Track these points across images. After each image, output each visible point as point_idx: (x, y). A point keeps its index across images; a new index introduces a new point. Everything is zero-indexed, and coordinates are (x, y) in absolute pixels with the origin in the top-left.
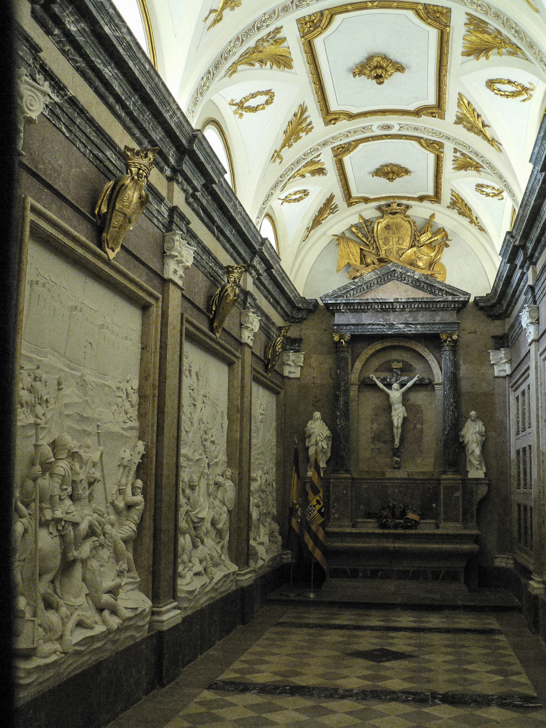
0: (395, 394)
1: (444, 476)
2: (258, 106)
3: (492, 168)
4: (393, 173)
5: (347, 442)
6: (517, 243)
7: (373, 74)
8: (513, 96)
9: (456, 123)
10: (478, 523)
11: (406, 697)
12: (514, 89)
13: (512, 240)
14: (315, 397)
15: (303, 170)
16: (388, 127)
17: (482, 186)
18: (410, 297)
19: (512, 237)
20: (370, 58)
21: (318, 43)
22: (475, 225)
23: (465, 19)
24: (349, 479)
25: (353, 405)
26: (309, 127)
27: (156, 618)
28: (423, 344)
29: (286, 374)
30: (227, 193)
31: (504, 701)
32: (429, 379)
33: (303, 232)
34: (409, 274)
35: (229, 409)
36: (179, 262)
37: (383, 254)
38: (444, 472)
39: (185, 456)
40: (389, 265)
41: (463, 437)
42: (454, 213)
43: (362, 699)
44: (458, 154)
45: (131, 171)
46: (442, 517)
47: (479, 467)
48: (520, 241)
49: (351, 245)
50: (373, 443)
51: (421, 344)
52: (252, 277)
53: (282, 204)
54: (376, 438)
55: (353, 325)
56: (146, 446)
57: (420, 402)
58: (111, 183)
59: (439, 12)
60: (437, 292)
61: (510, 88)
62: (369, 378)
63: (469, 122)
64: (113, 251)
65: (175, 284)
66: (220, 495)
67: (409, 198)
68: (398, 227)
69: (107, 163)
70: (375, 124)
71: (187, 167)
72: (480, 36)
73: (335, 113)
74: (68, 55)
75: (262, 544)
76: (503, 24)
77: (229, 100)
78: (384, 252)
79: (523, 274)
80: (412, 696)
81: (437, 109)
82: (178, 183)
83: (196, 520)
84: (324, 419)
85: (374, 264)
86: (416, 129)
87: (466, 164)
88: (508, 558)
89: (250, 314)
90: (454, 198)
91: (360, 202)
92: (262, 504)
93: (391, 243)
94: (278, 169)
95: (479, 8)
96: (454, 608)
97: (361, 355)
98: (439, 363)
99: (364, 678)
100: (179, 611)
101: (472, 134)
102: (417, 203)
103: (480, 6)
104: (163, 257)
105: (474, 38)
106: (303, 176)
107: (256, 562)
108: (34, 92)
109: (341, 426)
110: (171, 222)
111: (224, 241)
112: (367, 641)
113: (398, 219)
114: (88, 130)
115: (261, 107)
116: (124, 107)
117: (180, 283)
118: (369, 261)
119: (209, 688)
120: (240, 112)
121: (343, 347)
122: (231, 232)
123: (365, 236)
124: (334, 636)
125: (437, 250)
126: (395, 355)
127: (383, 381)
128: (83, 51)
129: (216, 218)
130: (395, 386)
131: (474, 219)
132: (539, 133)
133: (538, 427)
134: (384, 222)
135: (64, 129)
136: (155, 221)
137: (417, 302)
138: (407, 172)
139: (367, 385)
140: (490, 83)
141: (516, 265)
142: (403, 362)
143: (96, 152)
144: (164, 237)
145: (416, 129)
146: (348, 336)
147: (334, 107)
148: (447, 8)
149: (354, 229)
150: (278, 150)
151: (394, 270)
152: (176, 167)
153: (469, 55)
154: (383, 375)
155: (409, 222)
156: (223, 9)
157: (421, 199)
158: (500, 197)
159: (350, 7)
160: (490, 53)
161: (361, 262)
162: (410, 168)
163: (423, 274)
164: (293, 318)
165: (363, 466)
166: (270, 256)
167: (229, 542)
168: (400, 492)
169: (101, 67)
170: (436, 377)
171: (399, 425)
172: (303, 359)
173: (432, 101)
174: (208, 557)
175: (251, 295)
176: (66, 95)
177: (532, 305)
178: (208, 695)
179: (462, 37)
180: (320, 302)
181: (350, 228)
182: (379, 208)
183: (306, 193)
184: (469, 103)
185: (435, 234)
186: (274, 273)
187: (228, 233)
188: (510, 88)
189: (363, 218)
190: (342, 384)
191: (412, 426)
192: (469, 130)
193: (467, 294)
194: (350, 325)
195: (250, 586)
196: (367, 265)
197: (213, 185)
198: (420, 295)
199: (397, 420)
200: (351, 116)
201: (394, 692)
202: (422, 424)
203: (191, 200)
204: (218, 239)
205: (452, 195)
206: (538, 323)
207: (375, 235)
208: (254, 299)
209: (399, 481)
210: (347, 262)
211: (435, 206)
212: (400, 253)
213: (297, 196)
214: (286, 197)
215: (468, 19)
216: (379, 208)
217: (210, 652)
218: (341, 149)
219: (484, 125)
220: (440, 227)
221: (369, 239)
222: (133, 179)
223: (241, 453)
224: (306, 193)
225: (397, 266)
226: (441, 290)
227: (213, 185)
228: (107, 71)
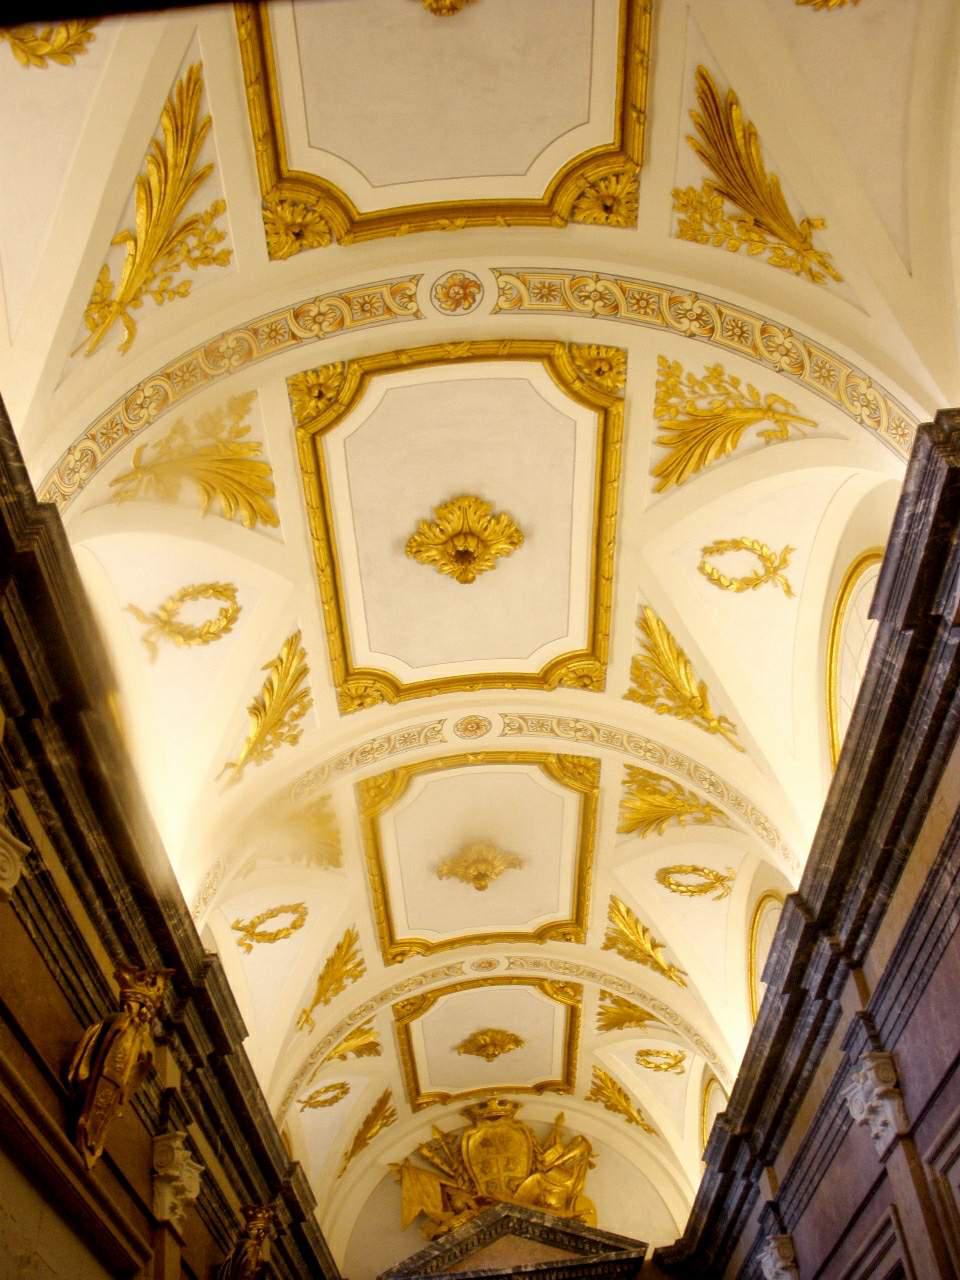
2: (279, 932)
3: (673, 1016)
4: (495, 1045)
6: (738, 1131)
7: (473, 872)
8: (701, 891)
9: (606, 947)
12: (702, 880)
13: (727, 1128)
15: (344, 1045)
16: (490, 965)
17: (648, 1053)
18: (541, 1261)
19: (727, 1121)
20: (466, 848)
21: (387, 824)
22: (637, 1123)
23: (622, 774)
26: (359, 969)
30: (244, 1072)
34: (534, 1220)
36: (179, 1191)
37: (482, 1191)
40: (498, 1208)
42: (598, 1109)
44: (608, 1002)
45: (130, 1007)
48: (742, 1127)
49: (424, 1178)
53: (302, 1110)
58: (97, 1027)
59: (581, 766)
60: (587, 1247)
61: (694, 880)
63: (629, 943)
64: (93, 1153)
65: (173, 1232)
67: (519, 1090)
68: (504, 1141)
69: (83, 996)
70: (467, 962)
71: (190, 1020)
72: (650, 798)
73: (403, 944)
74: (39, 807)
76: (690, 775)
77: (232, 921)
79: (748, 1188)
81: (573, 928)
82: (173, 1049)
85: (469, 1208)
86: (537, 964)
87: (623, 1015)
90: (597, 1081)
91: (435, 1102)
93: (495, 1170)
94: (307, 1043)
95: (648, 754)
101: (634, 964)
102: (534, 1097)
103: (649, 750)
104: (152, 1180)
105: (638, 804)
106: (343, 1057)
108: (7, 850)
110: (164, 1117)
111: (231, 1167)
113: (501, 1127)
114: (61, 935)
115: (285, 933)
116: (108, 903)
117: (179, 1230)
118: (459, 1204)
120: (248, 942)
123: (446, 1161)
125: (575, 1176)
128: (64, 801)
131: (635, 1114)
132: (779, 929)
134: (477, 1136)
135: (30, 926)
136: (142, 1112)
137: (554, 1269)
138: (517, 1042)
140: (663, 876)
141: (734, 1173)
143: (69, 973)
144: (152, 1143)
145: (537, 964)
147: (401, 934)
148: (593, 759)
149: (425, 1152)
150: (308, 1009)
151: (507, 1217)
152: (174, 1020)
153: (629, 831)
155: (524, 1132)
156: (246, 761)
157: (540, 1088)
158: (679, 1070)
159: (440, 764)
160: (664, 826)
161: (445, 1208)
162: (522, 1034)
163: (560, 1219)
169: (85, 831)
173: (564, 913)
176: (38, 867)
177: (779, 1235)
179: (618, 802)
182: (467, 1112)
183: (344, 1089)
184: (628, 911)
185: (569, 1147)
187: (238, 1150)
188: (694, 880)
192: (629, 956)
193: (644, 1245)
196: (457, 1212)
197: (226, 1057)
198: (558, 1256)
200: (429, 948)
203: (188, 1083)
205: (596, 1076)
206: (797, 1267)
210: (419, 1209)
212: (513, 1185)
213: (330, 1095)
214: (311, 1098)
215: (629, 775)
216: (467, 1112)
218: (408, 1007)
219: (654, 945)
220: (576, 1134)
221: (455, 1166)
222: (132, 1021)
224: (344, 1089)
225: (512, 1208)
226: (593, 1243)
227: (226, 1057)
228: (91, 838)
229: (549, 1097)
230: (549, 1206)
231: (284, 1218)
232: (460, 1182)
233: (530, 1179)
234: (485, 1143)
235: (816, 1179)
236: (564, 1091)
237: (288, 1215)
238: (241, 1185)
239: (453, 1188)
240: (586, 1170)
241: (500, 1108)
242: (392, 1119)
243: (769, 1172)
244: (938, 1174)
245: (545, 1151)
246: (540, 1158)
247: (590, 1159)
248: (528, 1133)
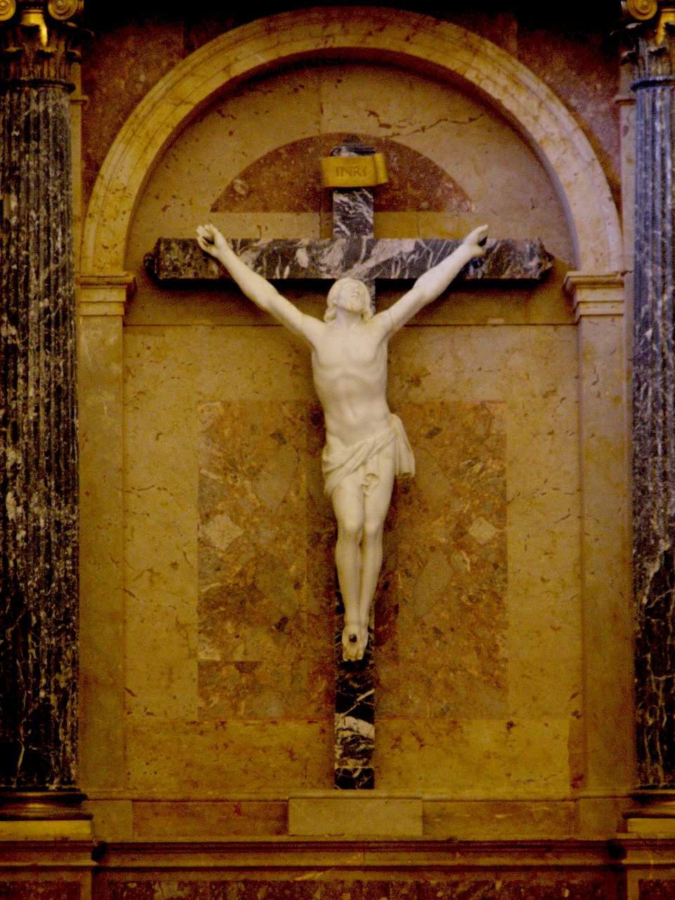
0: (347, 341)
1: (641, 827)
5: (67, 626)
24: (75, 846)
25: (96, 409)
28: (513, 45)
32: (546, 256)
38: (642, 802)
50: (209, 631)
51: (498, 41)
54: (231, 603)
57: (485, 391)
62: (188, 245)
97: (142, 108)
98: (605, 158)
109: (33, 537)
121: (42, 57)
126: (346, 107)
127: (273, 260)
130: (349, 291)
139: (179, 283)
142: (388, 147)
154: (275, 226)
165: (153, 774)
170: (585, 245)
171: (374, 526)
190: (37, 284)
191: (438, 531)
199: (359, 499)
202: (500, 515)
209: (371, 859)
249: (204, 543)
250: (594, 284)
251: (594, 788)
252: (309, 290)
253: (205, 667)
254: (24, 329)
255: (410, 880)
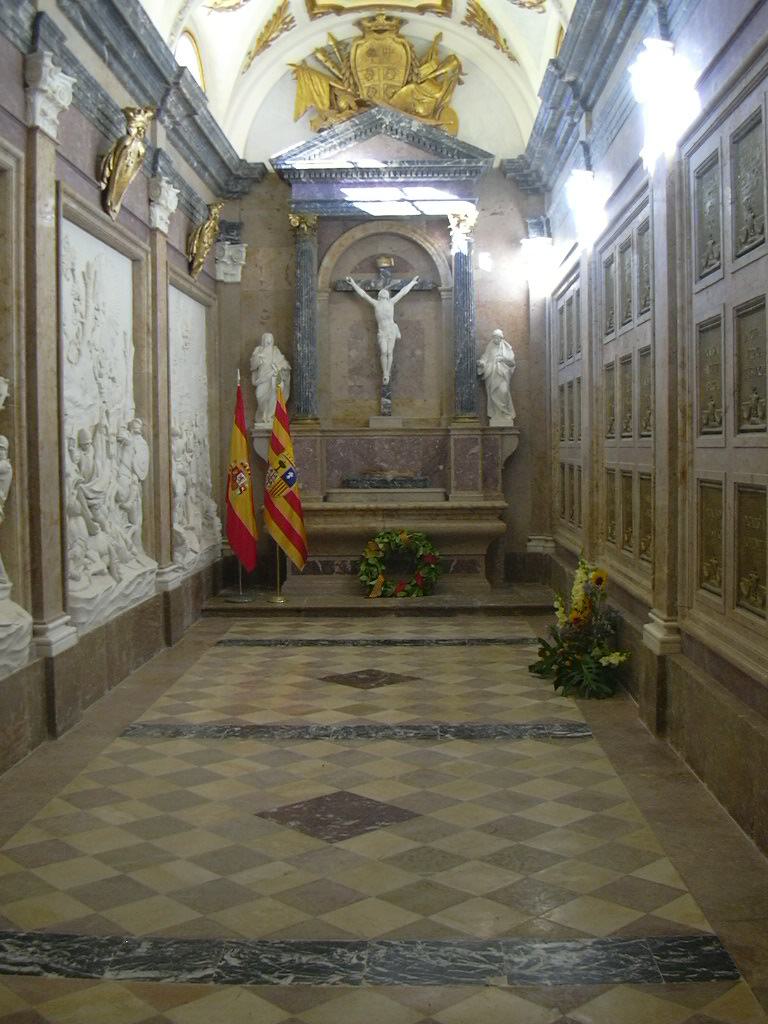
0: (385, 306)
1: (454, 425)
5: (313, 377)
10: (504, 490)
11: (406, 733)
14: (265, 311)
22: (503, 51)
27: (40, 639)
29: (220, 277)
31: (542, 732)
33: (241, 58)
34: (402, 124)
35: (136, 330)
37: (364, 95)
39: (71, 400)
40: (373, 111)
41: (482, 366)
42: (471, 33)
43: (344, 738)
46: (453, 483)
47: (505, 411)
49: (316, 79)
52: (166, 127)
54: (355, 371)
55: (320, 201)
56: (11, 386)
60: (445, 153)
65: (44, 134)
66: (127, 459)
67: (404, 9)
75: (192, 529)
78: (365, 92)
79: (573, 125)
80: (415, 732)
83: (91, 495)
84: (277, 344)
85: (350, 108)
88: (547, 541)
89: (163, 184)
90: (470, 9)
92: (189, 468)
93: (376, 78)
96: (471, 611)
99: (345, 710)
100: (74, 629)
107: (184, 556)
109: (304, 355)
110: (35, 37)
111: (120, 69)
112: (349, 661)
113: (388, 40)
118: (342, 104)
119: (123, 734)
122: (130, 55)
123: (336, 66)
124: (300, 656)
125: (445, 87)
129: (106, 34)
130: (384, 293)
131: (502, 41)
133: (590, 351)
134: (365, 45)
136: (10, 35)
146: (312, 220)
151: (380, 119)
154: (365, 277)
155: (404, 45)
157: (422, 9)
158: (540, 10)
161: (332, 106)
163: (425, 126)
164: (229, 192)
166: (191, 95)
167: (143, 526)
168: (393, 449)
171: (391, 352)
172: (244, 255)
174: (112, 549)
175: (164, 155)
178: (124, 744)
180: (269, 167)
181: (314, 54)
182: (358, 24)
185: (441, 64)
186: (199, 121)
189: (333, 38)
190: (304, 292)
191: (407, 353)
193: (490, 156)
194: (315, 201)
195: (177, 591)
196: (340, 111)
201: (388, 728)
204: (110, 65)
205: (470, 5)
207: (352, 65)
208: (169, 162)
209: (390, 433)
211: (443, 22)
216: (358, 24)
217: (124, 686)
220: (450, 53)
221: (343, 71)
223: (156, 395)
229: (429, 17)
230: (417, 114)
231: (178, 111)
232: (346, 85)
233: (405, 88)
234: (371, 53)
235: (615, 132)
236: (442, 13)
237: (182, 109)
238: (131, 84)
239: (340, 89)
240: (454, 87)
241: (386, 22)
242: (292, 25)
243: (587, 116)
244: (683, 157)
245: (421, 66)
246: (416, 71)
247: (461, 77)
248: (408, 48)
249: (349, 356)
250: (444, 291)
251: (445, 416)
252: (374, 293)
253: (351, 387)
254: (302, 303)
255: (399, 438)
